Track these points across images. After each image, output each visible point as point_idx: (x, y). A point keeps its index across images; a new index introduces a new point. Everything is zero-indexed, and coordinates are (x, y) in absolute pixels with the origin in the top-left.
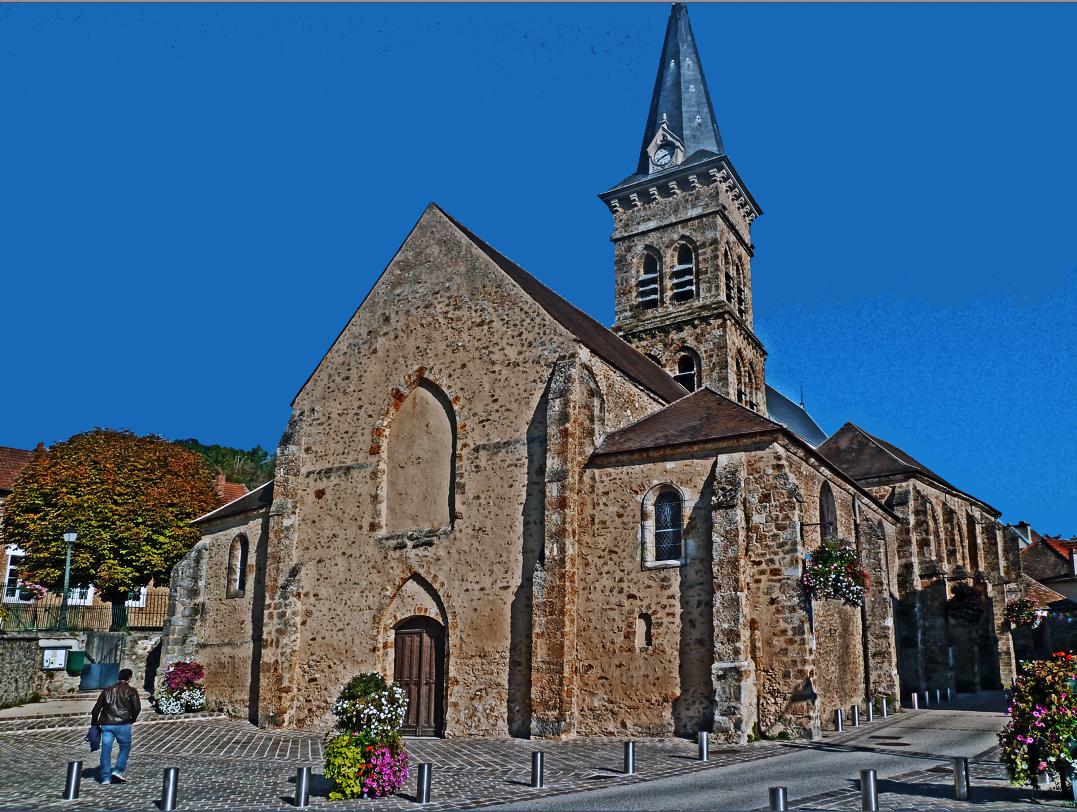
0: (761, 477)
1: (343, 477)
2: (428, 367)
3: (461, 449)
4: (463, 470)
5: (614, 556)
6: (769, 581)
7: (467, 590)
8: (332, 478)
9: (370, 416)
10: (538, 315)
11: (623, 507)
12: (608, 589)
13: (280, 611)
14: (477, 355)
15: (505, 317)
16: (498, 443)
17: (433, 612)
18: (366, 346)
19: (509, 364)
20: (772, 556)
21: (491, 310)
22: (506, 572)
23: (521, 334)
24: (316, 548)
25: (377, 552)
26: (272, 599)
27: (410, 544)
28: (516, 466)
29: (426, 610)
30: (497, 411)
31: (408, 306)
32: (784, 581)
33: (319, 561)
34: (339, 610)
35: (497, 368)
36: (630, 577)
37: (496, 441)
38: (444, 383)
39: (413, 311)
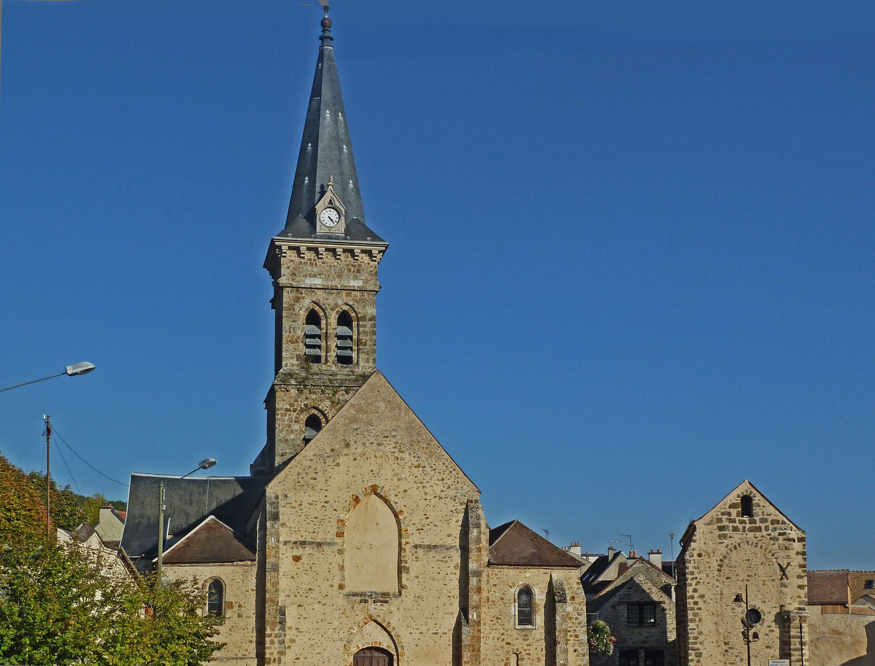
0: (571, 587)
2: (380, 486)
4: (407, 559)
5: (499, 620)
6: (574, 640)
7: (411, 633)
8: (307, 549)
9: (335, 510)
10: (454, 470)
12: (496, 638)
13: (281, 639)
14: (415, 486)
15: (433, 466)
16: (429, 545)
17: (386, 643)
18: (331, 460)
19: (435, 497)
20: (576, 628)
21: (424, 459)
22: (436, 624)
23: (443, 479)
24: (296, 596)
25: (345, 604)
26: (273, 630)
27: (370, 601)
28: (442, 561)
29: (380, 644)
30: (429, 525)
31: (365, 440)
34: (317, 640)
35: (428, 497)
36: (508, 633)
37: (428, 544)
38: (392, 499)
39: (368, 444)
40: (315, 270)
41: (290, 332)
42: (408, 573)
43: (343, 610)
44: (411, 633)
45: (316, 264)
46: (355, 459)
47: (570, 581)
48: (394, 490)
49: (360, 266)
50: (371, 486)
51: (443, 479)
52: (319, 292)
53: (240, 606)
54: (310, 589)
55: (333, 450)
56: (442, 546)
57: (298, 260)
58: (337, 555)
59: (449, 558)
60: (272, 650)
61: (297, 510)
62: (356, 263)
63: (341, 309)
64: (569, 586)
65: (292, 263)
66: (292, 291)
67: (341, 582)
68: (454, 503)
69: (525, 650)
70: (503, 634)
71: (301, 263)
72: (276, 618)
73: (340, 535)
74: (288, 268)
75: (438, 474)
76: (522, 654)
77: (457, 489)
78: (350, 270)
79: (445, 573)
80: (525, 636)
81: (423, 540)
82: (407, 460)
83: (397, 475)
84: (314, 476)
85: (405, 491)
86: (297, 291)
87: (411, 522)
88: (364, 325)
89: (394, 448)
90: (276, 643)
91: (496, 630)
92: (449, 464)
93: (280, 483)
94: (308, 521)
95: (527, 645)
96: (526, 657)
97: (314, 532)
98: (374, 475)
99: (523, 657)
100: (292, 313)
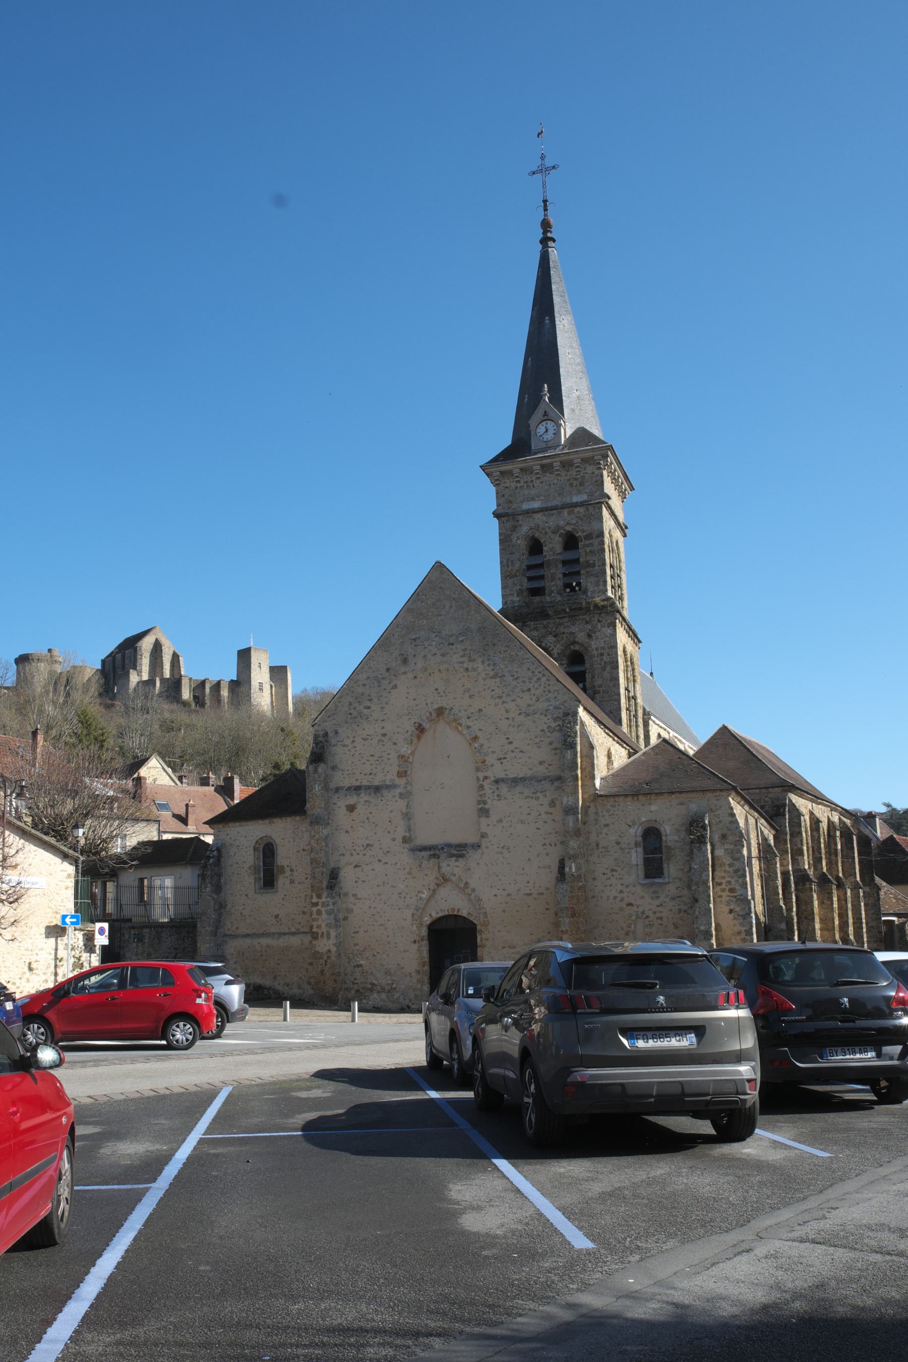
1: (373, 794)
2: (448, 707)
3: (483, 781)
5: (614, 873)
7: (495, 895)
8: (362, 795)
9: (395, 744)
10: (544, 675)
11: (620, 836)
13: (329, 908)
15: (515, 674)
18: (386, 682)
19: (520, 714)
22: (529, 882)
23: (529, 690)
24: (352, 855)
28: (532, 798)
29: (459, 910)
30: (513, 752)
33: (356, 866)
35: (511, 715)
37: (513, 776)
40: (533, 492)
41: (508, 566)
42: (488, 817)
43: (408, 869)
44: (495, 895)
45: (533, 486)
46: (415, 677)
47: (719, 812)
48: (466, 710)
49: (582, 477)
50: (436, 710)
51: (529, 690)
53: (292, 870)
55: (388, 670)
56: (531, 778)
57: (513, 485)
59: (541, 792)
60: (320, 923)
63: (564, 530)
65: (507, 490)
67: (405, 834)
68: (545, 719)
69: (655, 913)
70: (621, 892)
71: (517, 488)
72: (322, 883)
73: (402, 774)
74: (503, 496)
75: (522, 684)
76: (651, 919)
77: (548, 700)
78: (571, 485)
79: (538, 813)
80: (654, 892)
81: (506, 773)
82: (480, 670)
84: (368, 704)
86: (513, 519)
87: (490, 750)
88: (591, 544)
89: (462, 656)
90: (324, 913)
91: (611, 885)
92: (536, 668)
93: (329, 717)
95: (658, 906)
97: (370, 774)
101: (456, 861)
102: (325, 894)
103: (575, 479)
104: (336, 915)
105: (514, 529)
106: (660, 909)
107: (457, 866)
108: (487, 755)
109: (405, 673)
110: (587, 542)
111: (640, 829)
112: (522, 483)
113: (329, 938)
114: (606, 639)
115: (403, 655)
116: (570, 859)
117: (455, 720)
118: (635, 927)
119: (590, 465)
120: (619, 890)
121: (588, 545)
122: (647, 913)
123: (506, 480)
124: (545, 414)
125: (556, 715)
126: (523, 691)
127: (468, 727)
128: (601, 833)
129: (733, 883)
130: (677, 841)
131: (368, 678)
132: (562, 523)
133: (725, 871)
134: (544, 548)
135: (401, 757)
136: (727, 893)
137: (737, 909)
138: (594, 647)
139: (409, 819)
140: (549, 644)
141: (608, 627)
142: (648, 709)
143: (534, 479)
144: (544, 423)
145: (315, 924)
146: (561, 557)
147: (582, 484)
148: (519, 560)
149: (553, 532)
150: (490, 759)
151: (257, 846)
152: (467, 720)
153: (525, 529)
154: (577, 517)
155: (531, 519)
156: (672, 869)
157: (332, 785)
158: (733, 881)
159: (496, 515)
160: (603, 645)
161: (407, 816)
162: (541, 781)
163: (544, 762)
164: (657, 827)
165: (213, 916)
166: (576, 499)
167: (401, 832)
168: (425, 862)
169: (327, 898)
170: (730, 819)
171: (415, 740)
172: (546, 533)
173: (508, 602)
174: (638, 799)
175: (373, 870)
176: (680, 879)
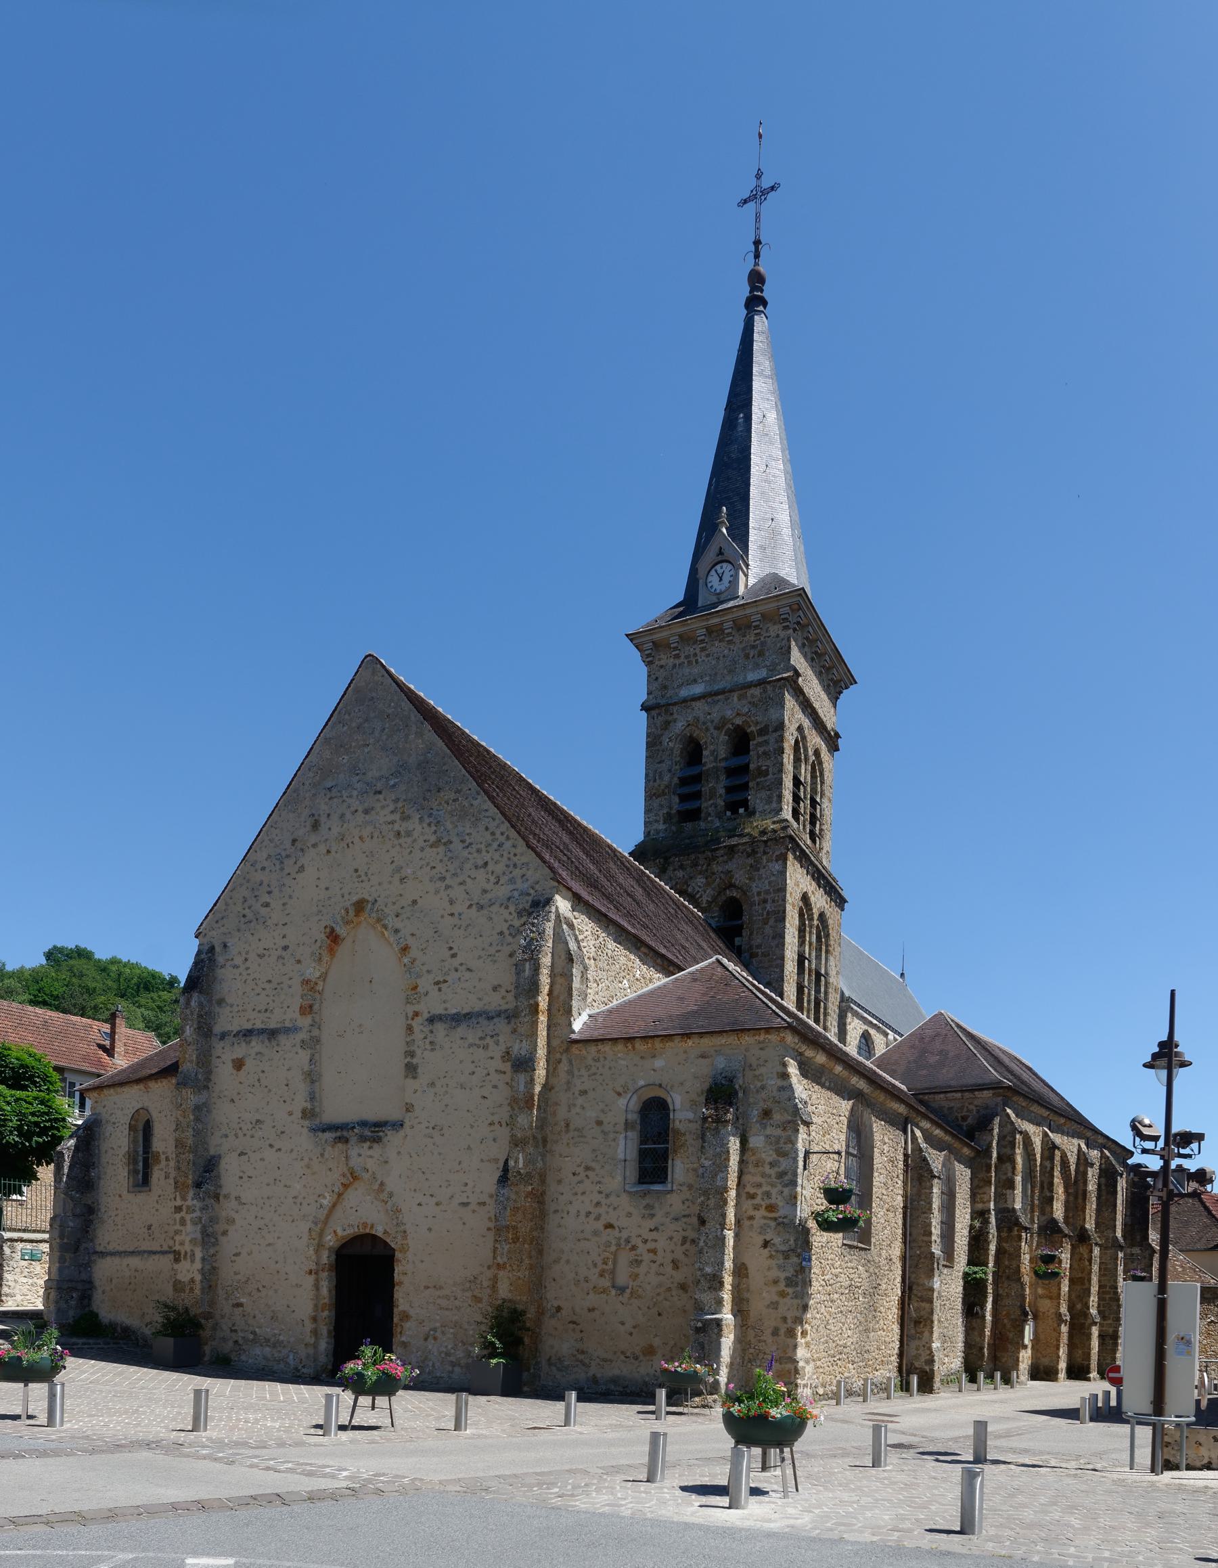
3: (413, 1019)
5: (590, 1173)
9: (299, 962)
11: (603, 1111)
12: (583, 1213)
28: (479, 1047)
30: (456, 970)
32: (781, 1220)
37: (454, 1011)
41: (655, 781)
42: (415, 1078)
45: (697, 662)
49: (763, 644)
52: (698, 704)
54: (258, 1121)
56: (479, 1014)
58: (300, 1051)
59: (492, 1036)
61: (241, 969)
62: (758, 642)
63: (733, 724)
64: (759, 1084)
66: (659, 714)
69: (646, 1241)
70: (598, 1204)
71: (674, 666)
74: (657, 679)
78: (747, 656)
79: (486, 1072)
80: (647, 1207)
83: (399, 869)
85: (415, 902)
87: (425, 968)
88: (765, 741)
91: (583, 1193)
94: (258, 990)
95: (651, 1230)
96: (647, 1257)
98: (360, 879)
99: (640, 1258)
100: (658, 750)
101: (370, 1148)
102: (191, 1194)
103: (753, 647)
104: (204, 1226)
105: (667, 725)
106: (654, 1235)
107: (371, 1157)
108: (419, 976)
109: (314, 846)
110: (760, 739)
111: (635, 1098)
112: (682, 659)
113: (193, 1261)
114: (773, 878)
115: (313, 815)
116: (517, 1145)
117: (379, 920)
118: (615, 1263)
119: (774, 624)
120: (595, 1201)
121: (760, 744)
122: (634, 1241)
123: (662, 656)
124: (721, 553)
125: (521, 907)
126: (476, 867)
127: (397, 931)
128: (575, 1105)
129: (774, 1196)
130: (690, 1121)
131: (269, 856)
132: (729, 713)
133: (763, 1175)
134: (704, 753)
135: (306, 982)
136: (762, 1212)
137: (777, 1240)
138: (755, 890)
139: (313, 1082)
140: (697, 889)
141: (777, 861)
142: (847, 994)
143: (698, 651)
144: (718, 567)
145: (177, 1238)
146: (723, 764)
147: (761, 654)
148: (670, 771)
149: (717, 728)
150: (425, 984)
151: (133, 1123)
152: (396, 920)
153: (679, 726)
154: (750, 703)
155: (689, 711)
156: (680, 1168)
157: (217, 1029)
158: (774, 1192)
159: (645, 707)
160: (767, 887)
161: (312, 1077)
162: (493, 1018)
163: (500, 986)
164: (663, 1096)
165: (71, 1224)
166: (752, 676)
167: (301, 1102)
168: (329, 1149)
169: (193, 1199)
170: (780, 1083)
171: (326, 958)
172: (707, 729)
173: (652, 832)
174: (634, 1048)
175: (262, 1160)
176: (690, 1187)
